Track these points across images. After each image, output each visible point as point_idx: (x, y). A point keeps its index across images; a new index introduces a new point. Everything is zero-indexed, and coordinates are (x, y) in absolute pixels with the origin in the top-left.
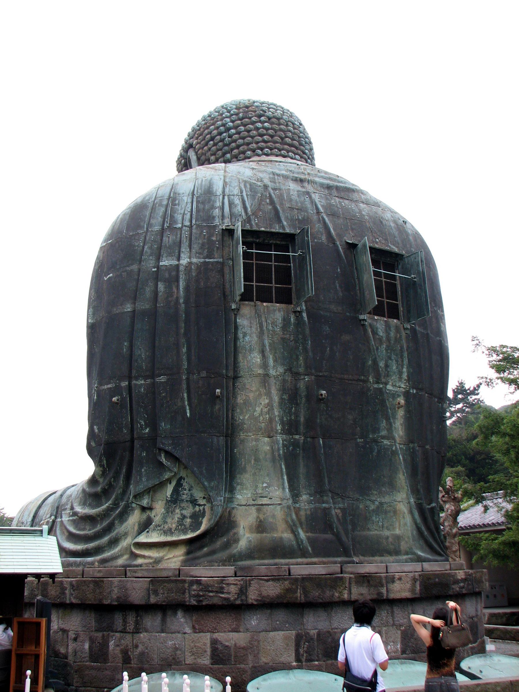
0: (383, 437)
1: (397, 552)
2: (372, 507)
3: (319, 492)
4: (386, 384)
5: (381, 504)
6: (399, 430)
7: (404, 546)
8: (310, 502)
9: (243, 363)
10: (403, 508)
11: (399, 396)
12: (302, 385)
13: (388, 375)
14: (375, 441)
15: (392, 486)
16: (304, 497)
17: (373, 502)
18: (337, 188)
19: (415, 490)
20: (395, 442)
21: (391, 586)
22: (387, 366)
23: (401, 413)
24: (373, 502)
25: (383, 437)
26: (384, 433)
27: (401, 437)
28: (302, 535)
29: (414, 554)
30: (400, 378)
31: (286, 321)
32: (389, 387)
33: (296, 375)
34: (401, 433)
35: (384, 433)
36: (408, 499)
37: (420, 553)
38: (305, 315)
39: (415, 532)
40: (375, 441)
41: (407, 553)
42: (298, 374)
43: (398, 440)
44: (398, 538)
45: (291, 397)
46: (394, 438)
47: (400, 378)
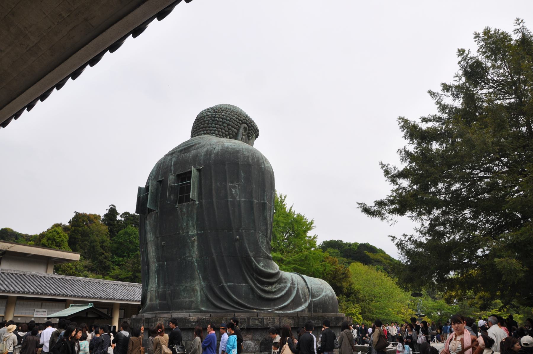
0: (188, 257)
1: (190, 308)
2: (182, 288)
3: (164, 285)
4: (188, 232)
5: (186, 287)
6: (195, 253)
7: (194, 305)
8: (162, 288)
9: (147, 238)
10: (198, 288)
11: (195, 236)
12: (159, 242)
13: (188, 228)
14: (184, 259)
15: (193, 278)
16: (161, 286)
17: (183, 286)
18: (185, 149)
19: (205, 279)
20: (193, 258)
21: (156, 323)
22: (187, 224)
23: (196, 244)
24: (183, 286)
25: (188, 257)
26: (188, 255)
27: (197, 255)
28: (158, 301)
29: (199, 309)
30: (194, 228)
31: (155, 217)
32: (190, 233)
33: (157, 238)
34: (197, 253)
35: (188, 255)
36: (200, 283)
37: (203, 309)
38: (159, 214)
39: (204, 299)
40: (184, 259)
41: (194, 309)
42: (157, 238)
43: (194, 255)
44: (192, 302)
45: (158, 247)
46: (192, 256)
47: (194, 228)
